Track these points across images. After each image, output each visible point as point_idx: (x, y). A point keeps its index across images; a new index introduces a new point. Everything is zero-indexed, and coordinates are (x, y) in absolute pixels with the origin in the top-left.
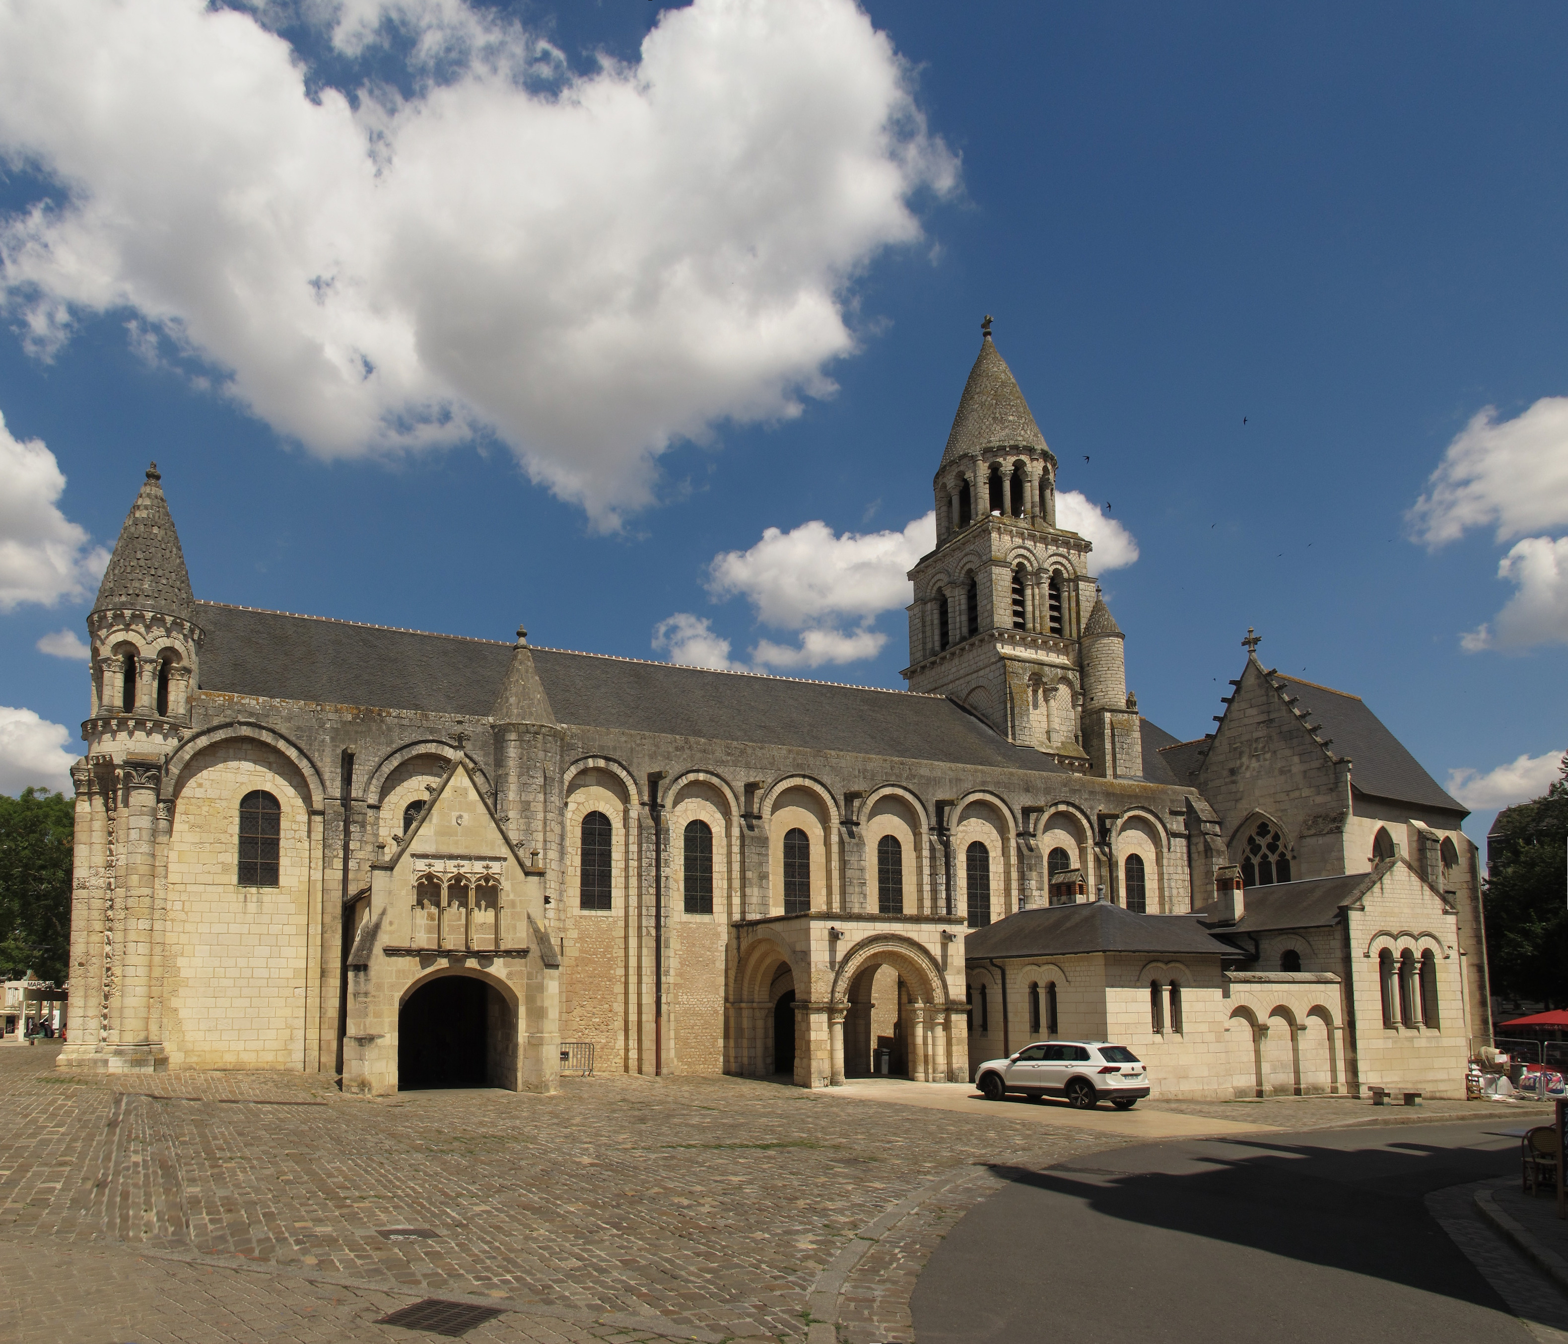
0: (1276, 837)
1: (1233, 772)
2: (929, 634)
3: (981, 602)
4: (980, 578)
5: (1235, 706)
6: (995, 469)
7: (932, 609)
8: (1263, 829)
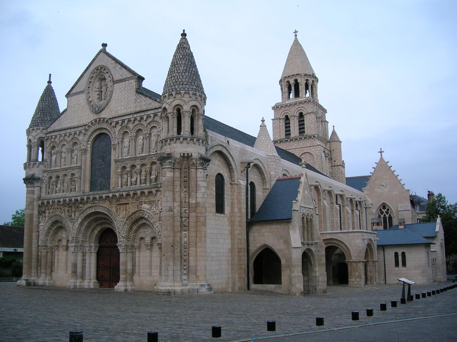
0: (388, 210)
6: (307, 80)
7: (282, 123)
8: (384, 207)
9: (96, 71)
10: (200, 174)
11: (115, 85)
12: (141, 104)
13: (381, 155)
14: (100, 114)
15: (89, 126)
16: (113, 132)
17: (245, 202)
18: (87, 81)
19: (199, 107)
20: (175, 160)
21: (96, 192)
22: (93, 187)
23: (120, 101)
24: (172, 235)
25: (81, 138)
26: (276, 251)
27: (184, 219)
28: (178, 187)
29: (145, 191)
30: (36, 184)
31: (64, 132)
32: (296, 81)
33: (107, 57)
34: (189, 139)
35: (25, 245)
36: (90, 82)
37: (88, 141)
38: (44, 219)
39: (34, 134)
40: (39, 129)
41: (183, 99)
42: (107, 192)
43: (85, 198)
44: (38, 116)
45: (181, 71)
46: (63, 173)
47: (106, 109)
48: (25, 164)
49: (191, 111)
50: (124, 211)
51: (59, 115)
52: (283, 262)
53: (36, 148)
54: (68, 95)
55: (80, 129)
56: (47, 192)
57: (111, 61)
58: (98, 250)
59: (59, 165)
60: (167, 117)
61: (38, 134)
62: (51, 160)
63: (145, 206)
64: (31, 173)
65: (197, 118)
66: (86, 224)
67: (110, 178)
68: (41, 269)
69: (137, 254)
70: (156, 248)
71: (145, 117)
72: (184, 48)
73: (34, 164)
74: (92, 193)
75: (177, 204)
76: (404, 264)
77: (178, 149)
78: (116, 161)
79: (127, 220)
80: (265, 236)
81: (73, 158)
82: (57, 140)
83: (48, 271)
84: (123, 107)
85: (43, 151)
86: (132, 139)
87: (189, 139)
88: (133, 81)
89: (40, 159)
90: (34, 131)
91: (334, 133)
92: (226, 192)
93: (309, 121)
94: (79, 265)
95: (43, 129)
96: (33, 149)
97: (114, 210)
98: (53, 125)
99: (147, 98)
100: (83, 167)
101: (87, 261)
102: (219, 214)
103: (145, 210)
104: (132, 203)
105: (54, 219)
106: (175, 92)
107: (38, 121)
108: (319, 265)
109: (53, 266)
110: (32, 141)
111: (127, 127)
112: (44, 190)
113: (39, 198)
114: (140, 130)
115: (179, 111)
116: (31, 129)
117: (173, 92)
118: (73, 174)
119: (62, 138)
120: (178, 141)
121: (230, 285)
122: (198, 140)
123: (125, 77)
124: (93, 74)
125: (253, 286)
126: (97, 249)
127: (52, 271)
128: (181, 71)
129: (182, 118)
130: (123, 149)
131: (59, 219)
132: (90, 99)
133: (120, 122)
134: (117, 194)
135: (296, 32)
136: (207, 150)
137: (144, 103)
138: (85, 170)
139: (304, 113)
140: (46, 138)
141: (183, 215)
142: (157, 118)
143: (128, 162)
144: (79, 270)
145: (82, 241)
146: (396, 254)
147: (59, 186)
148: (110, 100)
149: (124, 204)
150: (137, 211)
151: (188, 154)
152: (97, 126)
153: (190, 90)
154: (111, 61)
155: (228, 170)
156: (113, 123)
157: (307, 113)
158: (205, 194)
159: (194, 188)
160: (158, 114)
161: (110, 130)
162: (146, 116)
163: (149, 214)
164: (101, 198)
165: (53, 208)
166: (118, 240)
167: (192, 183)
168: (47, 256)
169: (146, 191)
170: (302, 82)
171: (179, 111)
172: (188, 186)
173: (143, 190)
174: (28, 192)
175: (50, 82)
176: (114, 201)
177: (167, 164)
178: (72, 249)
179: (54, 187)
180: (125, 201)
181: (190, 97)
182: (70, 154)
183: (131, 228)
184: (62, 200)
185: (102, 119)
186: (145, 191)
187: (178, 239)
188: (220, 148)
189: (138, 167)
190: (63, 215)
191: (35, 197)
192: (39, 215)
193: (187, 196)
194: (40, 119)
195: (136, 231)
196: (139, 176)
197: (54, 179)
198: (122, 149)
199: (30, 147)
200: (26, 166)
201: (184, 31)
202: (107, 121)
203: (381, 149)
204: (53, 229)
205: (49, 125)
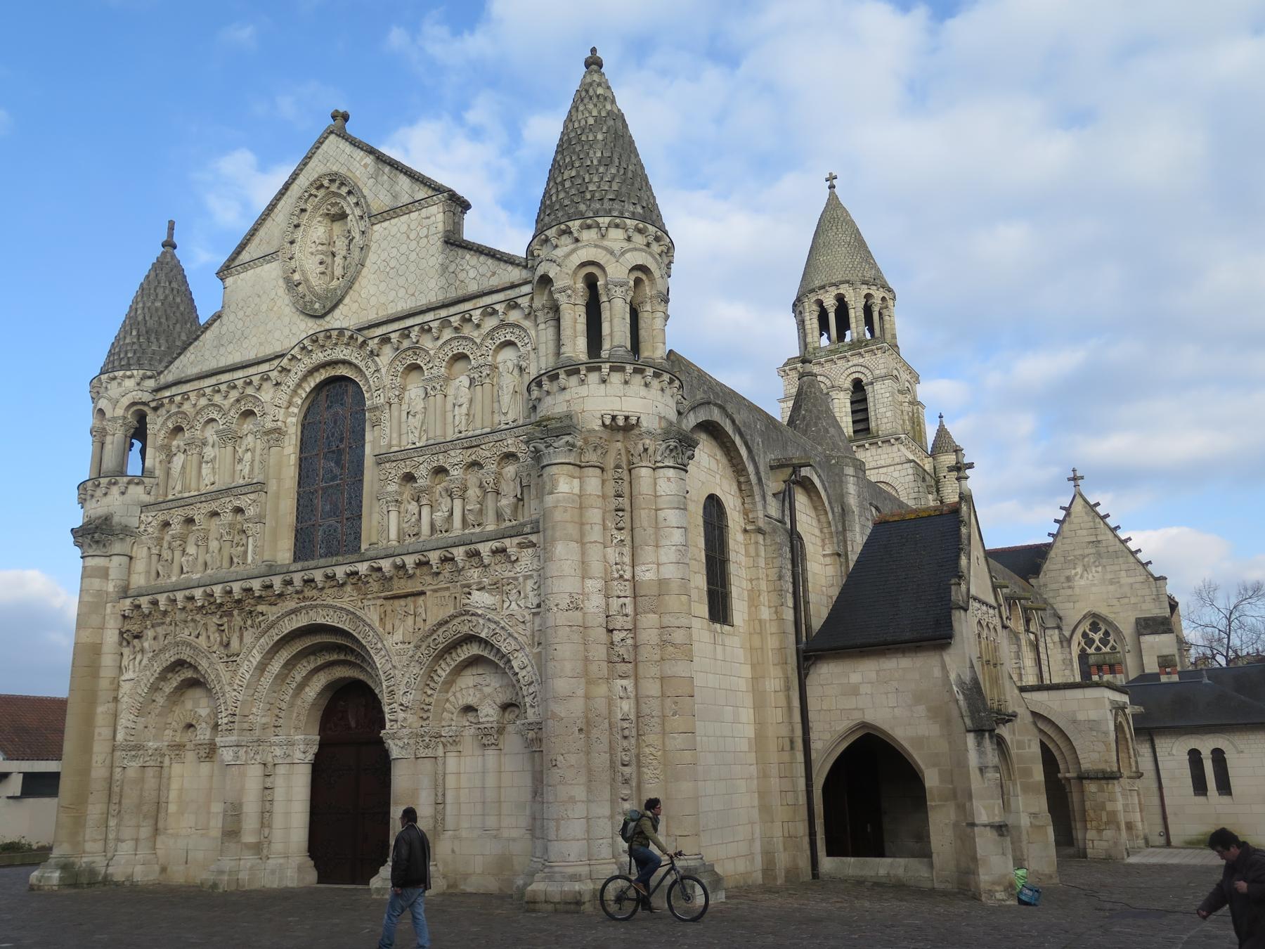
1: (1068, 579)
5: (1066, 526)
6: (868, 296)
9: (314, 191)
10: (667, 483)
11: (376, 227)
12: (462, 276)
14: (328, 318)
15: (294, 357)
16: (372, 370)
17: (791, 590)
18: (284, 225)
19: (657, 273)
20: (586, 441)
21: (312, 563)
22: (304, 548)
23: (392, 273)
24: (580, 692)
25: (267, 395)
26: (906, 745)
27: (617, 636)
28: (598, 529)
29: (480, 547)
30: (117, 547)
31: (213, 381)
33: (348, 148)
34: (629, 368)
35: (68, 746)
36: (297, 226)
37: (290, 404)
38: (139, 657)
39: (114, 390)
40: (130, 377)
41: (605, 243)
42: (355, 557)
43: (277, 582)
44: (128, 341)
45: (595, 162)
46: (207, 508)
47: (346, 301)
48: (82, 486)
49: (632, 283)
50: (410, 620)
51: (197, 332)
52: (931, 779)
53: (120, 435)
54: (225, 271)
55: (264, 367)
56: (154, 574)
57: (362, 159)
58: (317, 755)
59: (193, 485)
60: (555, 309)
61: (129, 389)
62: (168, 473)
63: (481, 599)
64: (98, 508)
65: (648, 308)
66: (276, 666)
67: (360, 517)
68: (118, 825)
69: (452, 762)
70: (512, 741)
71: (476, 315)
72: (598, 96)
73: (110, 483)
74: (299, 565)
75: (593, 585)
76: (1224, 786)
77: (596, 399)
78: (380, 459)
79: (418, 647)
80: (877, 694)
81: (240, 460)
82: (187, 407)
83: (145, 832)
84: (402, 292)
85: (143, 452)
86: (434, 388)
87: (629, 368)
88: (434, 209)
89: (134, 467)
90: (115, 383)
91: (942, 433)
92: (732, 556)
93: (881, 401)
94: (251, 808)
95: (144, 378)
96: (109, 439)
97: (372, 616)
98: (177, 363)
99: (482, 258)
100: (272, 486)
101: (279, 794)
102: (718, 626)
103: (480, 612)
104: (435, 591)
105: (169, 657)
106: (578, 223)
107: (130, 355)
108: (1027, 789)
109: (162, 815)
110: (108, 415)
111: (416, 349)
112: (140, 566)
113: (124, 592)
114: (462, 357)
115: (591, 282)
116: (104, 377)
117: (570, 224)
118: (238, 510)
119: (203, 401)
120: (593, 377)
121: (758, 860)
122: (657, 375)
123: (405, 199)
124: (306, 201)
125: (828, 864)
126: (315, 749)
127: (156, 831)
128: (595, 162)
129: (605, 307)
130: (406, 416)
131: (186, 655)
132: (296, 277)
133: (393, 336)
134: (386, 564)
136: (679, 413)
137: (472, 273)
138: (277, 496)
139: (865, 381)
140: (153, 404)
141: (619, 622)
142: (514, 316)
143: (421, 459)
144: (250, 824)
145: (264, 727)
146: (1195, 756)
147: (191, 549)
148: (359, 273)
149: (405, 596)
150: (453, 617)
151: (627, 418)
152: (319, 357)
153: (626, 215)
154: (362, 159)
155: (735, 487)
156: (370, 342)
157: (876, 379)
158: (674, 556)
159: (651, 531)
160: (519, 301)
161: (361, 365)
162: (479, 312)
163: (493, 626)
164: (330, 577)
165: (168, 620)
166: (387, 716)
167: (644, 516)
168: (142, 780)
169: (485, 549)
171: (591, 282)
172: (628, 526)
173: (472, 547)
174: (86, 574)
175: (170, 244)
176: (375, 586)
177: (558, 454)
178: (227, 755)
179: (177, 554)
180: (411, 587)
181: (629, 239)
182: (229, 449)
183: (431, 673)
184: (198, 593)
185: (334, 333)
186: (480, 547)
187: (601, 704)
188: (716, 415)
189: (455, 473)
190: (201, 640)
191: (111, 588)
192: (121, 644)
193: (627, 559)
194: (135, 347)
195: (449, 682)
196: (458, 503)
197: (176, 528)
198: (400, 422)
199: (99, 435)
200: (85, 492)
201: (594, 50)
202: (351, 337)
204: (168, 688)
205: (164, 364)
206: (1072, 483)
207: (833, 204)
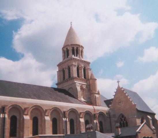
0: (125, 118)
2: (61, 77)
3: (71, 71)
4: (71, 68)
7: (62, 73)
8: (123, 116)
13: (118, 84)
32: (67, 49)
135: (71, 23)
170: (70, 49)
203: (118, 80)
206: (118, 83)
207: (71, 27)
